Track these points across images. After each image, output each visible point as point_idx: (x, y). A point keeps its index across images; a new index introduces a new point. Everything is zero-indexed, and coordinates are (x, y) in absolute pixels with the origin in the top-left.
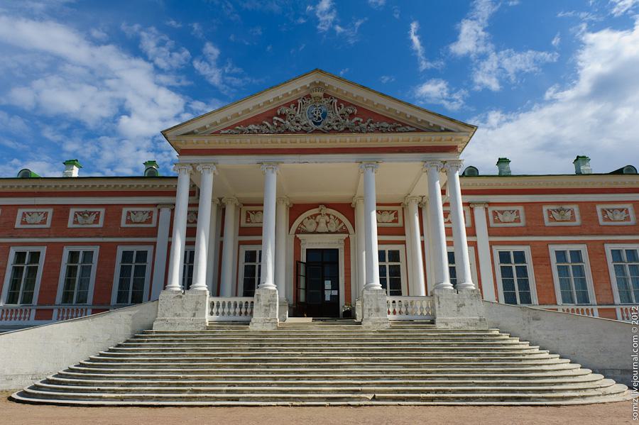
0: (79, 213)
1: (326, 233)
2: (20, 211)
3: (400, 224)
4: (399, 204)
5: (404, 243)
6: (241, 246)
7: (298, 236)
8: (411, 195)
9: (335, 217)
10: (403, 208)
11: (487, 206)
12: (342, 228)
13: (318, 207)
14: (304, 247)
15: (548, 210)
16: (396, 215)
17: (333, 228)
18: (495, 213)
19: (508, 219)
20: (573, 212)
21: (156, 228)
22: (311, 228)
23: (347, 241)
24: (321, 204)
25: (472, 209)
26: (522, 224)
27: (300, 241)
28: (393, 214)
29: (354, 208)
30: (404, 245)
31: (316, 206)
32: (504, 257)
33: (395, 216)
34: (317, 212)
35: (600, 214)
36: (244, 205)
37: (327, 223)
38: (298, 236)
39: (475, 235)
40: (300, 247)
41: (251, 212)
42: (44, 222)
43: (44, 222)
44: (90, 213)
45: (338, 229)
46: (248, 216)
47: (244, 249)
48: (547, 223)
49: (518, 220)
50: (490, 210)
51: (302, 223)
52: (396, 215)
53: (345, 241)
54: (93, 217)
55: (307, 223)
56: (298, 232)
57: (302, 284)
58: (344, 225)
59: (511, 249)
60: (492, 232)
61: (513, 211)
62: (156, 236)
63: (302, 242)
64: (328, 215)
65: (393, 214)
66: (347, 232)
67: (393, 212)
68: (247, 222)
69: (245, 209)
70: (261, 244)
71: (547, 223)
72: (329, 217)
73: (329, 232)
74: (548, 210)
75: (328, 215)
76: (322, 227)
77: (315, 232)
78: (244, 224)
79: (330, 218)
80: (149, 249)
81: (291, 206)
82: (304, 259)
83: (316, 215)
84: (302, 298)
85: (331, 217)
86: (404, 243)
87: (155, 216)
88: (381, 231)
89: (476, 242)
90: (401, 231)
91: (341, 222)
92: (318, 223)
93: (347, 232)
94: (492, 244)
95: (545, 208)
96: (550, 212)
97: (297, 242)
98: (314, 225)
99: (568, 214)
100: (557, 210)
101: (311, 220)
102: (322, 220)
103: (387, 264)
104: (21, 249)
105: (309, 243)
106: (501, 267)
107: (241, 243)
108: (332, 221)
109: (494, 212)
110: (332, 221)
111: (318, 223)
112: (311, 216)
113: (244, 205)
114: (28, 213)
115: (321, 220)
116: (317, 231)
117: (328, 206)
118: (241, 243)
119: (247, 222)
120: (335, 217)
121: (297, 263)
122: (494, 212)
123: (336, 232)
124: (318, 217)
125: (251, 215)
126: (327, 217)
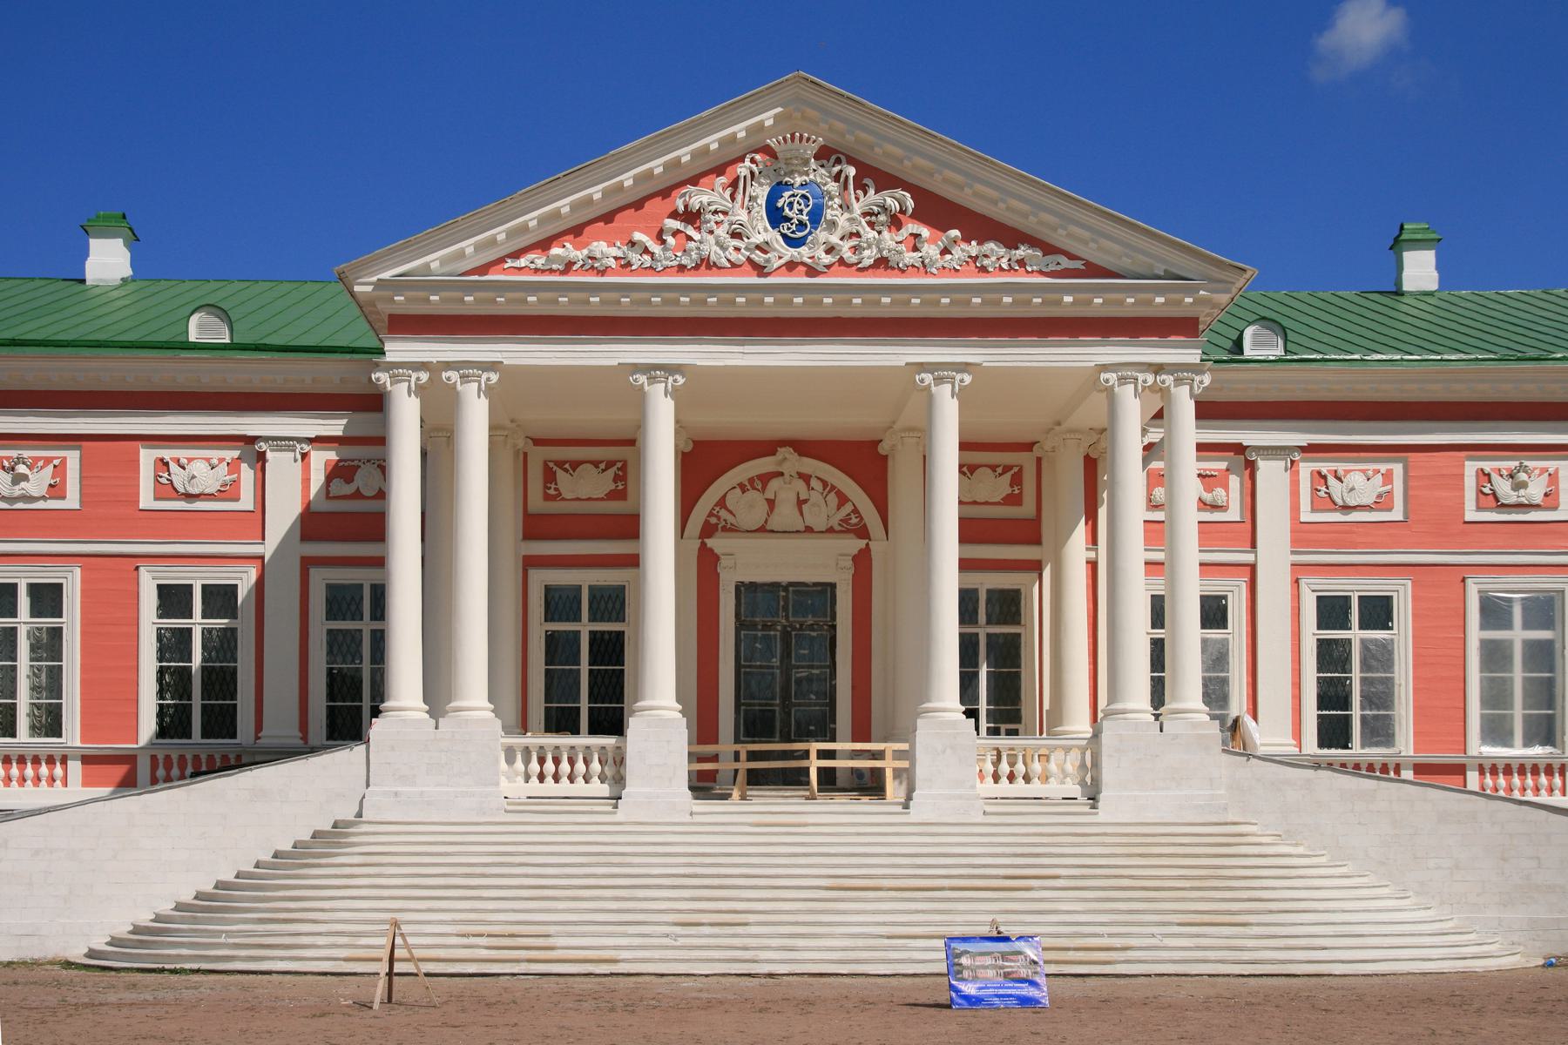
3: (1027, 509)
4: (1028, 447)
7: (710, 542)
9: (825, 484)
10: (1039, 460)
12: (846, 520)
13: (773, 453)
16: (1017, 480)
17: (819, 523)
23: (862, 562)
25: (1251, 466)
27: (717, 558)
28: (1008, 476)
29: (885, 458)
31: (767, 447)
32: (1332, 611)
33: (1011, 486)
36: (538, 442)
37: (801, 503)
38: (710, 542)
40: (718, 575)
41: (560, 464)
46: (549, 477)
47: (541, 578)
49: (1383, 503)
51: (722, 503)
55: (734, 499)
56: (708, 530)
58: (855, 511)
59: (1355, 588)
60: (1302, 535)
63: (724, 562)
64: (806, 478)
65: (1008, 476)
66: (862, 533)
67: (1007, 469)
68: (547, 497)
69: (538, 455)
72: (808, 483)
73: (809, 530)
75: (806, 478)
76: (786, 515)
77: (762, 530)
78: (537, 504)
79: (810, 488)
83: (766, 478)
85: (814, 483)
88: (970, 531)
89: (1253, 568)
91: (843, 499)
92: (771, 503)
93: (862, 533)
101: (752, 495)
102: (785, 492)
107: (530, 562)
110: (816, 497)
111: (771, 503)
112: (751, 481)
113: (538, 442)
115: (782, 496)
117: (803, 447)
118: (530, 562)
119: (547, 497)
120: (825, 484)
124: (774, 484)
125: (560, 474)
126: (800, 485)
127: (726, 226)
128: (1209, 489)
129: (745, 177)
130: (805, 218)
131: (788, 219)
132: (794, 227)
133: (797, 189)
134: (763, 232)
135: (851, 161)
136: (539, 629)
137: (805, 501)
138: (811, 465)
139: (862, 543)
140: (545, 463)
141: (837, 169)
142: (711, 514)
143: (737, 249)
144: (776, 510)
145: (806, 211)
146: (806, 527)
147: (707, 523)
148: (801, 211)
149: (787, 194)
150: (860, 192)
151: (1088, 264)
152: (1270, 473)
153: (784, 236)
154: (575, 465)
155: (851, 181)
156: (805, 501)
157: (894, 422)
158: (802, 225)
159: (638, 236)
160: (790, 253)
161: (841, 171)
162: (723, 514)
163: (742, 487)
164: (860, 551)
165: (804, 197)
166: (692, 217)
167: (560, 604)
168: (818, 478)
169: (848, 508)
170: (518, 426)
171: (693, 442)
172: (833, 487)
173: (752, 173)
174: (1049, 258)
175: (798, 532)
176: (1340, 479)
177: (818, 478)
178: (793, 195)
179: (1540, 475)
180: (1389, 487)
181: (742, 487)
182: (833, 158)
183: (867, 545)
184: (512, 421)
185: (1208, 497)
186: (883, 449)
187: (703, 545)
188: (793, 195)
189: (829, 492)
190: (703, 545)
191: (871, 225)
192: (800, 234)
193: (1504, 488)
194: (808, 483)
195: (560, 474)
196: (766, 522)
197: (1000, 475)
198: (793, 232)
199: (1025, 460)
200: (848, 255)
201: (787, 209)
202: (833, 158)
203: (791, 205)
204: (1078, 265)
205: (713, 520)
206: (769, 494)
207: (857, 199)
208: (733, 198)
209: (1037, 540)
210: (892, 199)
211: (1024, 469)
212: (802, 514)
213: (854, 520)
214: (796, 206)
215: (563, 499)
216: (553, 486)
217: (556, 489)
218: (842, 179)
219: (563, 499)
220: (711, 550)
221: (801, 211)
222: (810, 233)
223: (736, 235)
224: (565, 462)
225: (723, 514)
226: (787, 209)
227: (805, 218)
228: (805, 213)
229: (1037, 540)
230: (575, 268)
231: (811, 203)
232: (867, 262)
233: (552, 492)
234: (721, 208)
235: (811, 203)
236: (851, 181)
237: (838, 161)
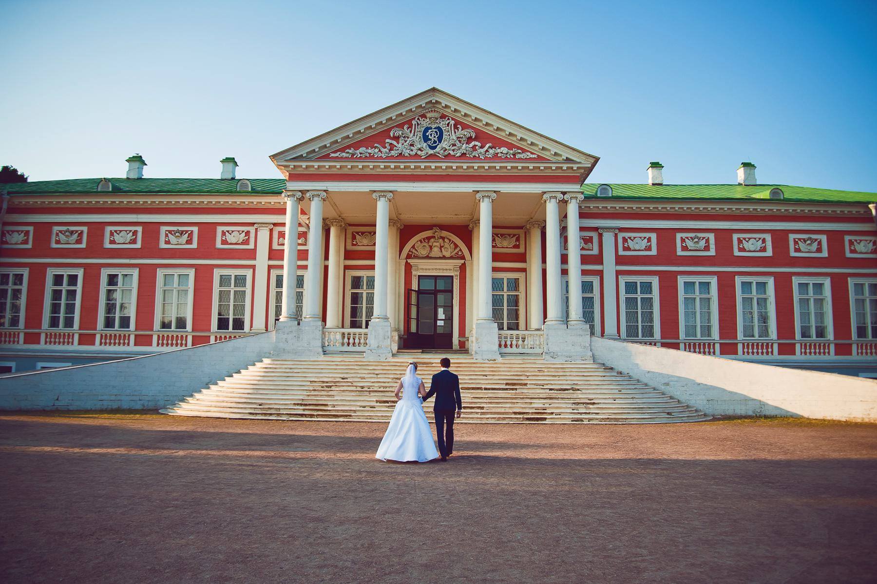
0: (170, 232)
1: (440, 258)
2: (109, 229)
3: (521, 250)
4: (521, 228)
5: (524, 270)
6: (346, 271)
7: (409, 261)
8: (533, 220)
9: (450, 240)
10: (525, 232)
11: (617, 231)
13: (432, 229)
14: (415, 273)
15: (682, 238)
16: (518, 240)
17: (448, 254)
18: (625, 240)
19: (639, 245)
20: (707, 241)
21: (254, 250)
22: (424, 252)
23: (463, 268)
24: (435, 226)
25: (600, 236)
26: (654, 252)
27: (411, 266)
28: (514, 238)
29: (471, 231)
30: (524, 273)
32: (631, 287)
34: (431, 235)
35: (735, 242)
36: (350, 225)
37: (441, 247)
38: (409, 261)
39: (602, 263)
41: (357, 233)
42: (134, 241)
43: (134, 241)
44: (182, 233)
45: (453, 254)
46: (354, 238)
48: (680, 252)
49: (649, 248)
50: (621, 235)
51: (413, 247)
52: (518, 240)
53: (460, 267)
54: (185, 237)
56: (409, 256)
57: (414, 314)
58: (461, 250)
60: (620, 260)
61: (645, 238)
62: (255, 259)
64: (443, 238)
65: (514, 238)
67: (514, 235)
68: (353, 245)
69: (351, 230)
70: (374, 269)
71: (680, 252)
72: (444, 241)
73: (444, 258)
74: (682, 238)
75: (443, 238)
76: (436, 252)
77: (428, 257)
78: (350, 247)
80: (249, 273)
81: (402, 228)
82: (415, 286)
83: (429, 238)
84: (413, 329)
85: (446, 240)
86: (524, 270)
87: (252, 235)
90: (522, 258)
91: (456, 246)
92: (431, 247)
93: (463, 258)
94: (618, 273)
95: (679, 236)
96: (683, 240)
97: (408, 268)
98: (428, 248)
99: (702, 243)
100: (691, 238)
103: (505, 294)
104: (113, 271)
105: (422, 269)
106: (626, 298)
107: (346, 268)
108: (447, 245)
109: (624, 238)
110: (447, 245)
111: (431, 247)
112: (424, 239)
113: (350, 225)
114: (116, 231)
116: (429, 256)
117: (443, 227)
118: (346, 268)
120: (450, 240)
121: (408, 291)
122: (624, 238)
123: (451, 258)
124: (432, 240)
125: (357, 236)
126: (441, 240)
127: (408, 142)
128: (586, 243)
129: (415, 125)
130: (436, 139)
132: (432, 142)
133: (434, 129)
135: (453, 119)
136: (349, 292)
137: (443, 246)
138: (445, 233)
139: (462, 261)
140: (353, 232)
141: (448, 121)
142: (410, 251)
143: (412, 150)
144: (433, 250)
146: (443, 256)
147: (408, 254)
148: (435, 137)
149: (430, 131)
150: (456, 130)
151: (538, 156)
152: (608, 238)
153: (429, 145)
154: (363, 233)
155: (452, 126)
156: (443, 246)
157: (474, 217)
158: (435, 142)
159: (375, 145)
160: (431, 152)
161: (449, 123)
162: (414, 251)
163: (421, 241)
164: (462, 264)
165: (436, 132)
166: (397, 138)
167: (357, 282)
168: (448, 238)
169: (458, 249)
170: (342, 218)
171: (404, 225)
172: (453, 242)
173: (418, 123)
174: (524, 154)
175: (440, 257)
176: (632, 240)
177: (448, 238)
178: (432, 131)
179: (702, 240)
180: (649, 243)
181: (421, 241)
182: (446, 119)
183: (465, 262)
184: (340, 217)
185: (586, 247)
186: (471, 226)
187: (407, 261)
188: (432, 131)
189: (451, 243)
190: (407, 261)
191: (460, 141)
192: (434, 145)
193: (690, 244)
194: (444, 241)
195: (357, 236)
196: (429, 254)
197: (512, 237)
199: (521, 232)
200: (452, 153)
201: (430, 136)
202: (446, 119)
203: (431, 135)
204: (535, 156)
205: (410, 253)
206: (430, 244)
207: (455, 132)
208: (411, 132)
209: (524, 261)
210: (467, 133)
211: (520, 236)
212: (442, 251)
213: (460, 253)
215: (359, 245)
216: (355, 241)
217: (356, 242)
218: (450, 126)
219: (359, 245)
220: (409, 263)
221: (435, 137)
222: (438, 144)
223: (412, 145)
224: (360, 232)
225: (414, 251)
226: (430, 136)
227: (436, 139)
229: (524, 261)
230: (355, 156)
231: (438, 133)
232: (458, 155)
233: (355, 243)
234: (407, 136)
235: (438, 133)
236: (452, 126)
237: (449, 119)
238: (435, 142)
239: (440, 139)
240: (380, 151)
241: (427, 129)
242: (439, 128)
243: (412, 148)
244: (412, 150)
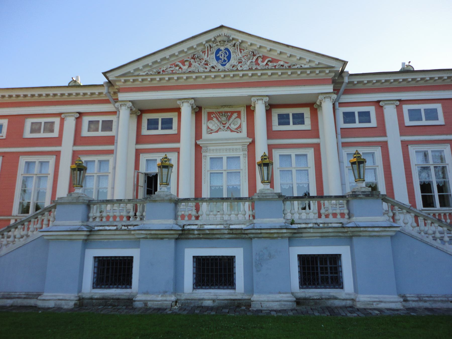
131: (221, 59)
134: (214, 62)
143: (206, 68)
145: (226, 57)
148: (224, 56)
158: (225, 61)
165: (225, 52)
192: (224, 63)
198: (223, 62)
201: (220, 56)
203: (221, 55)
214: (223, 55)
221: (224, 56)
223: (207, 64)
226: (220, 56)
227: (226, 59)
228: (226, 57)
238: (225, 61)
239: (229, 58)
240: (180, 68)
241: (219, 50)
242: (227, 49)
243: (206, 66)
244: (206, 68)
